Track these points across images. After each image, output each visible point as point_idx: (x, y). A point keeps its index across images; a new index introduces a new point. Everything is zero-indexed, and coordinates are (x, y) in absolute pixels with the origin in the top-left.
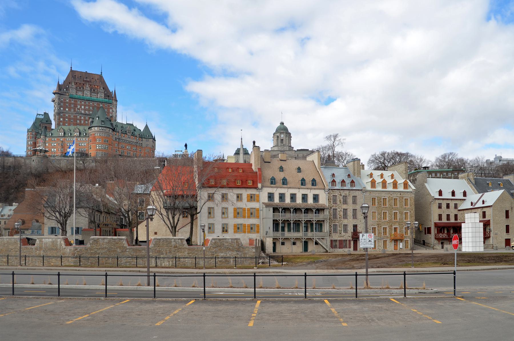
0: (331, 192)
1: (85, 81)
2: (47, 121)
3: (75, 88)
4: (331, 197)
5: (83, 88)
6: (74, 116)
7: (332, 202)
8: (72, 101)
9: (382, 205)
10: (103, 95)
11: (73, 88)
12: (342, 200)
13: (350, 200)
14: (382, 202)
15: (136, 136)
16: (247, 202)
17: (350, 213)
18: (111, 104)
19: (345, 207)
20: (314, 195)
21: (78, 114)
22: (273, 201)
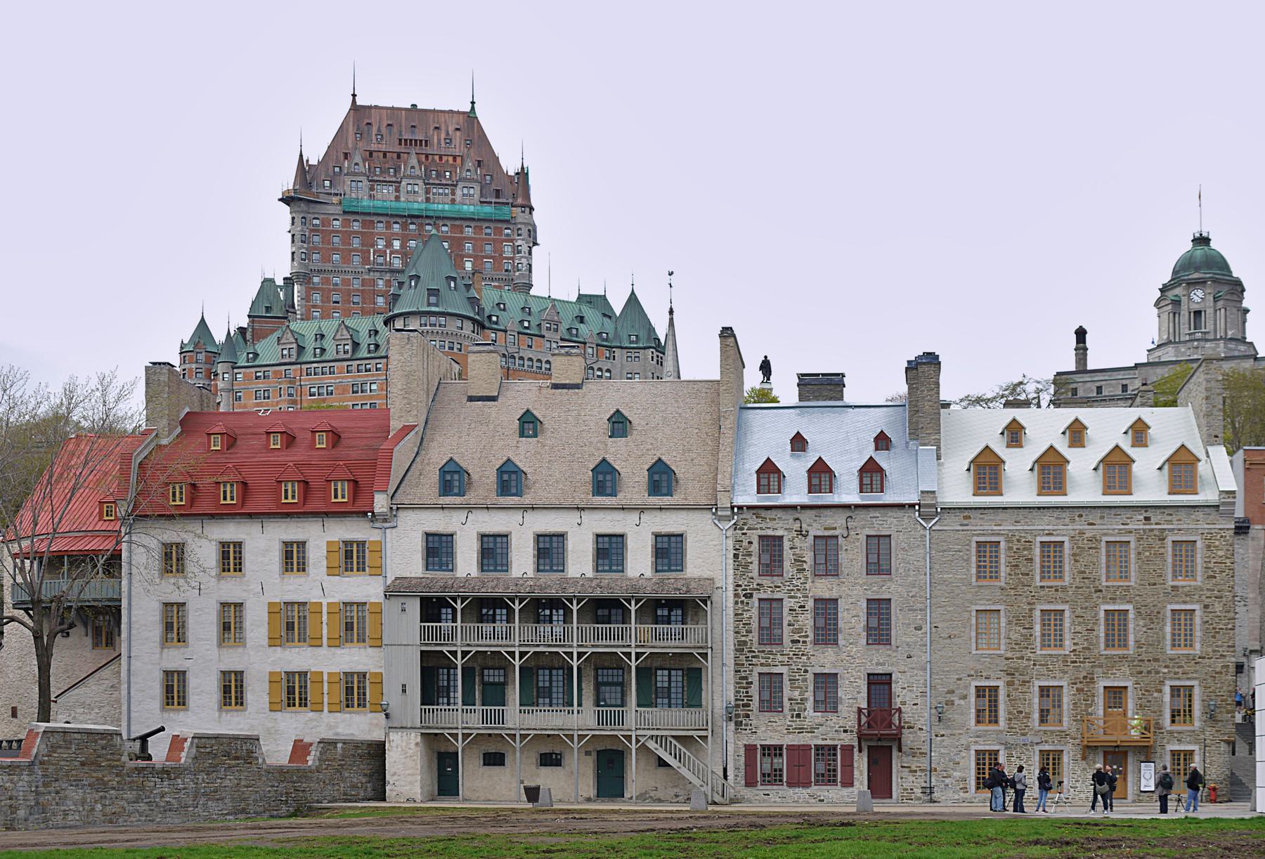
0: (753, 521)
1: (406, 144)
2: (268, 309)
3: (364, 175)
4: (750, 543)
5: (397, 170)
6: (364, 283)
7: (755, 567)
8: (355, 224)
9: (1038, 578)
10: (475, 191)
11: (355, 174)
12: (808, 557)
13: (853, 557)
14: (1037, 560)
15: (585, 343)
16: (326, 577)
17: (852, 619)
18: (507, 221)
19: (823, 588)
20: (657, 536)
21: (378, 274)
22: (563, 571)
